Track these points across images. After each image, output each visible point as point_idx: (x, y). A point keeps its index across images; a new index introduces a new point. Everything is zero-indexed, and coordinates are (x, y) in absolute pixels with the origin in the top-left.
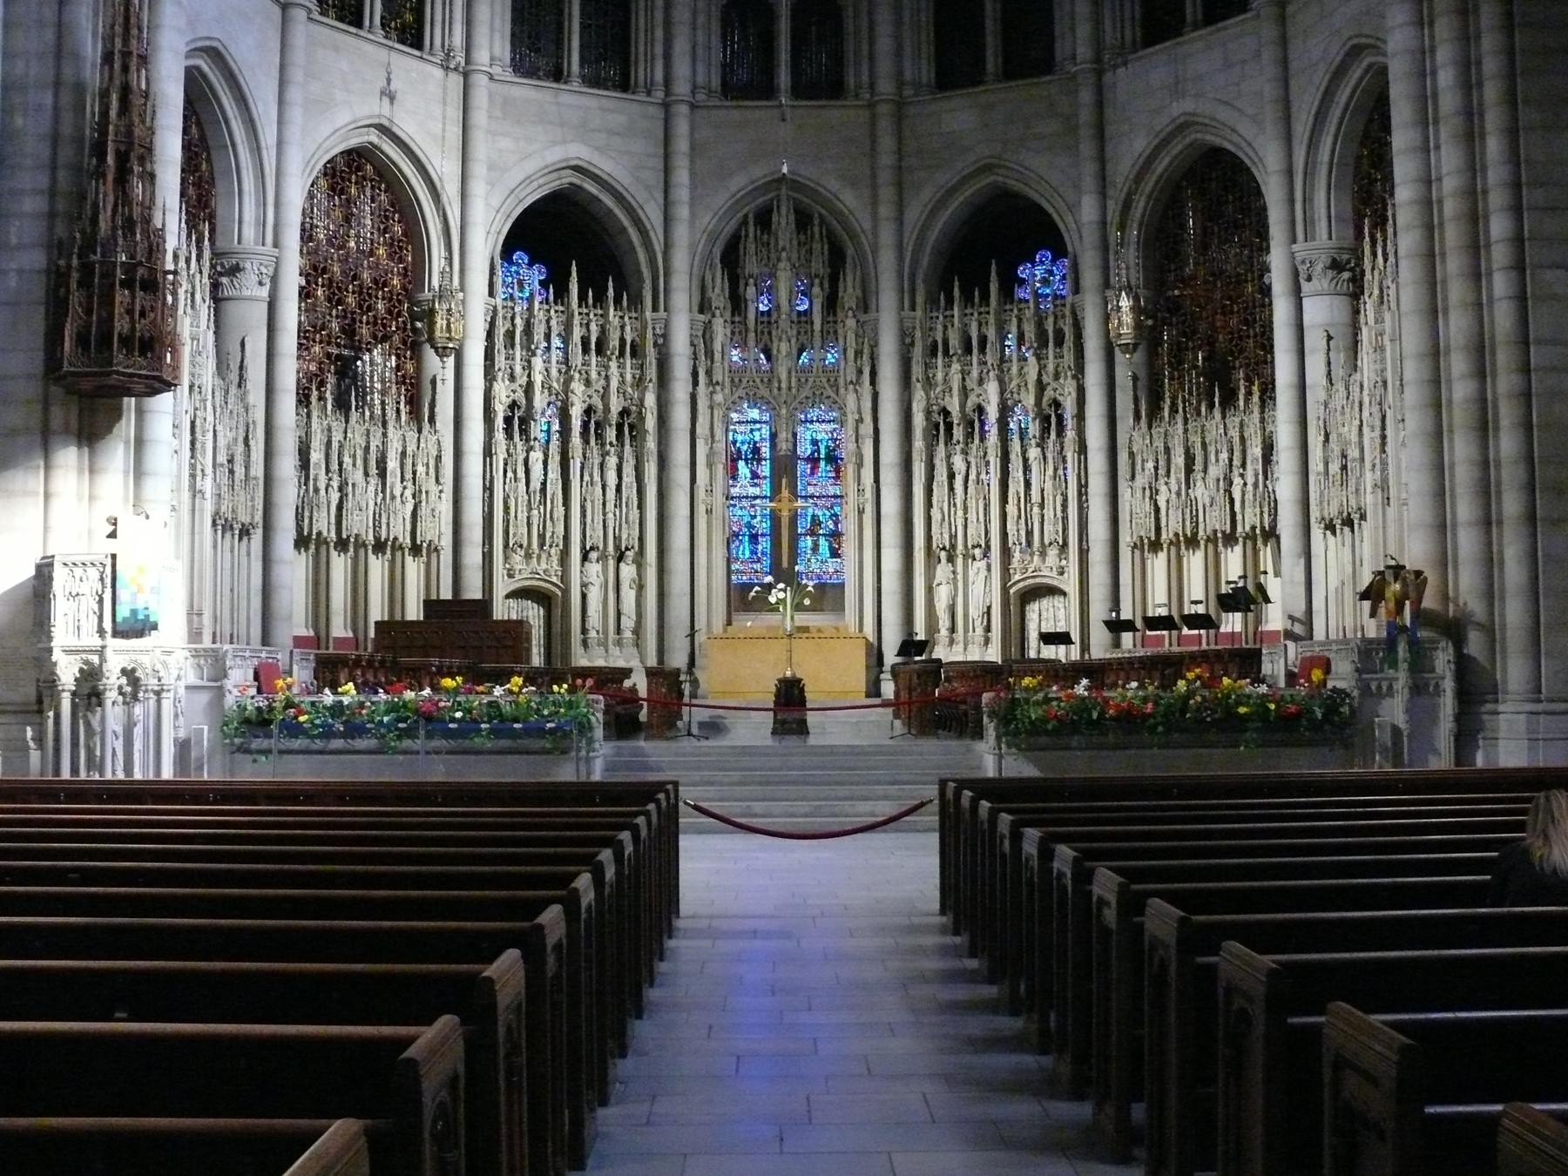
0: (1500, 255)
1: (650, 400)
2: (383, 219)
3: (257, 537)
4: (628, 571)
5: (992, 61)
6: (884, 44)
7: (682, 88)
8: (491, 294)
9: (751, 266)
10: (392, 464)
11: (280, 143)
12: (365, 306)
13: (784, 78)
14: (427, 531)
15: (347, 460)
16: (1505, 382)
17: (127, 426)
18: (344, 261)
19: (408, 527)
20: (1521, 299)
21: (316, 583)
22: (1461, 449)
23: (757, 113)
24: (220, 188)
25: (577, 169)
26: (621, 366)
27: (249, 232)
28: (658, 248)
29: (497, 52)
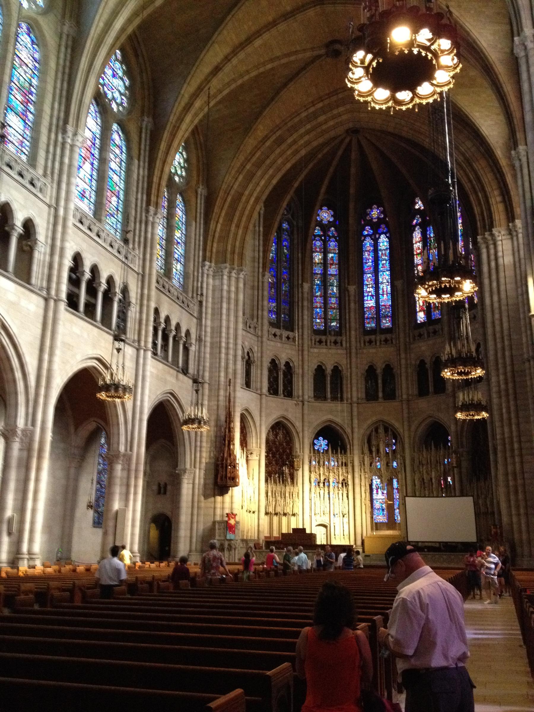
0: (516, 452)
1: (350, 477)
2: (285, 437)
3: (256, 513)
4: (346, 519)
5: (431, 389)
6: (404, 386)
7: (355, 399)
8: (310, 453)
9: (374, 442)
10: (287, 495)
11: (260, 425)
12: (281, 457)
13: (380, 395)
14: (295, 511)
15: (277, 494)
16: (520, 482)
17: (230, 492)
18: (276, 448)
19: (291, 509)
20: (522, 462)
21: (270, 523)
22: (512, 497)
23: (373, 405)
24: (248, 435)
25: (330, 421)
26: (342, 469)
27: (254, 445)
28: (350, 438)
29: (310, 395)
